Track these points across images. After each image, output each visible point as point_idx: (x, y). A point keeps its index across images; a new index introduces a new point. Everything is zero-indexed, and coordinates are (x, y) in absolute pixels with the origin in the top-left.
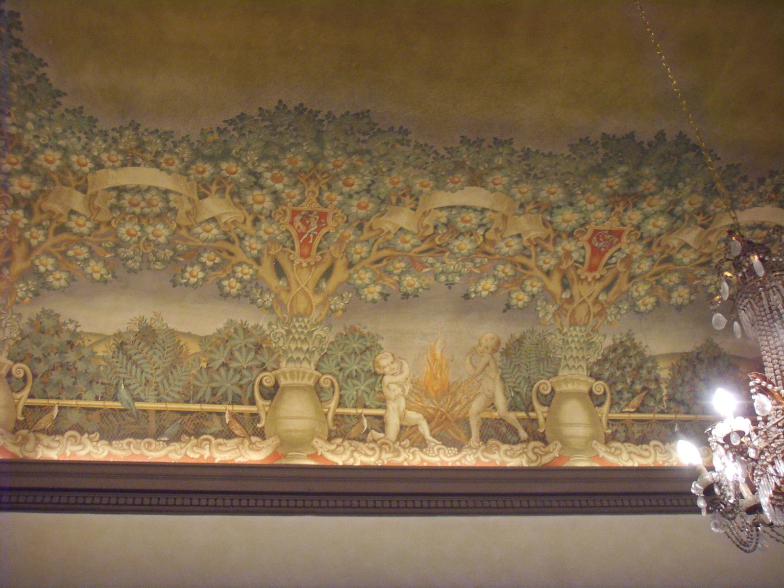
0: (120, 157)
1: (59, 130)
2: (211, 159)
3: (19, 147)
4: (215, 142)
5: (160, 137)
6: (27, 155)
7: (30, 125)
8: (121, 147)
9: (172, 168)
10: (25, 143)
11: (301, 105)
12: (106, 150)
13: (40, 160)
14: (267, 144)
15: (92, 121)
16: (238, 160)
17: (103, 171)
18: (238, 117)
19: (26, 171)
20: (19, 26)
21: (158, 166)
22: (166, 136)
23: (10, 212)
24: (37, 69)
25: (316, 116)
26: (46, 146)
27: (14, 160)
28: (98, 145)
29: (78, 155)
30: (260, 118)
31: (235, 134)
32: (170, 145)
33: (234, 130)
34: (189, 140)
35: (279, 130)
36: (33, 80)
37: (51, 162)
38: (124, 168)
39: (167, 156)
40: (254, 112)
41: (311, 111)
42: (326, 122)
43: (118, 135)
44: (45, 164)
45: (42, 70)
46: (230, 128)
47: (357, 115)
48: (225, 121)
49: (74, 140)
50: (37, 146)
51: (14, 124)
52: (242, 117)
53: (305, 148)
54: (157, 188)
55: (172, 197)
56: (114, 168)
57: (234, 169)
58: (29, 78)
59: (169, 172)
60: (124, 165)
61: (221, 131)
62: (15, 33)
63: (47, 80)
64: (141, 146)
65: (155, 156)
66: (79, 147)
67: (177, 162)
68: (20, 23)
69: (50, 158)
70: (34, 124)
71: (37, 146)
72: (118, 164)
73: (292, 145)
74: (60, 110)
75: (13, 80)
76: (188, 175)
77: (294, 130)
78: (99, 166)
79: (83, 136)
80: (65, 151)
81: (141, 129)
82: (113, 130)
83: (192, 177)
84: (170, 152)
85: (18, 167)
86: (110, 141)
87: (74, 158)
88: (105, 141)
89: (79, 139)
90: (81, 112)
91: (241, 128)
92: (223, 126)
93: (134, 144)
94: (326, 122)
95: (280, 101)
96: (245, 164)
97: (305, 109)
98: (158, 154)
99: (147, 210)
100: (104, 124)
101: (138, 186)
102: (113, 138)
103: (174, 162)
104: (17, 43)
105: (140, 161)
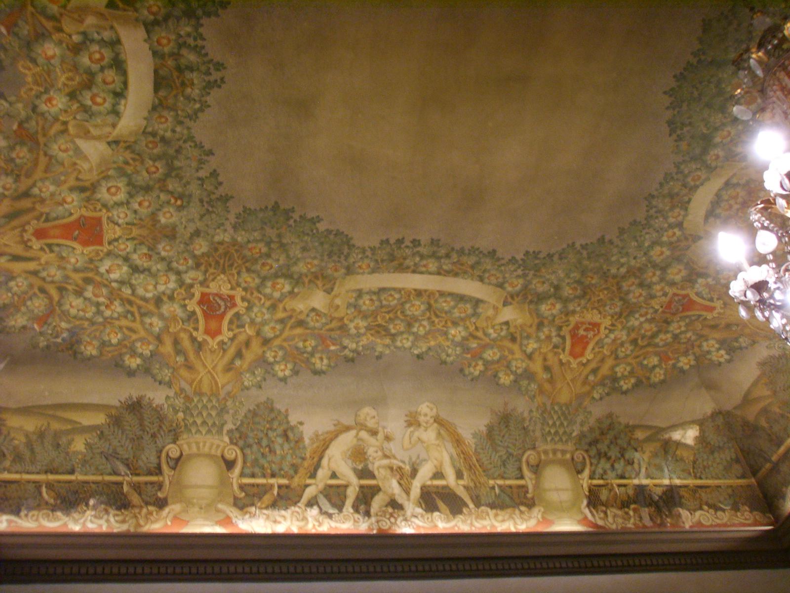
0: (677, 210)
1: (634, 244)
2: (705, 151)
3: (640, 269)
4: (689, 145)
5: (667, 183)
6: (649, 266)
7: (623, 260)
8: (667, 208)
9: (703, 177)
10: (638, 265)
11: (675, 76)
12: (665, 218)
13: (658, 260)
14: (709, 105)
15: (634, 223)
16: (716, 129)
17: (685, 225)
18: (669, 126)
19: (664, 269)
20: (536, 254)
21: (696, 187)
22: (668, 177)
23: (697, 286)
24: (576, 248)
25: (692, 65)
26: (645, 254)
27: (651, 274)
28: (658, 223)
29: (663, 236)
30: (677, 109)
31: (685, 129)
32: (680, 176)
33: (682, 129)
34: (679, 163)
35: (696, 94)
36: (585, 253)
37: (662, 253)
38: (689, 210)
39: (689, 179)
40: (669, 114)
41: (685, 69)
42: (703, 58)
43: (654, 210)
44: (661, 257)
45: (578, 245)
46: (679, 132)
47: (704, 31)
48: (670, 135)
49: (647, 236)
50: (644, 259)
51: (618, 269)
52: (670, 123)
53: (725, 76)
54: (720, 190)
55: (735, 181)
56: (686, 215)
57: (725, 133)
58: (581, 254)
59: (708, 179)
60: (686, 209)
61: (680, 139)
62: (541, 256)
63: (587, 244)
64: (671, 196)
65: (686, 187)
66: (655, 235)
67: (699, 173)
68: (534, 252)
69: (659, 253)
70: (622, 257)
71: (644, 259)
72: (682, 213)
73: (717, 86)
74: (616, 241)
75: (580, 263)
76: (716, 168)
77: (701, 83)
78: (680, 225)
79: (647, 230)
80: (654, 243)
81: (655, 193)
82: (648, 211)
83: (719, 164)
84: (686, 176)
85: (658, 273)
86: (659, 215)
87: (665, 239)
88: (657, 218)
89: (647, 233)
90: (623, 229)
91: (683, 124)
92: (674, 136)
93: (667, 200)
94: (703, 58)
95: (665, 93)
96: (723, 125)
97: (681, 74)
98: (685, 185)
99: (740, 200)
100: (640, 216)
101: (711, 202)
102: (656, 212)
103: (698, 175)
104: (550, 256)
105: (686, 199)
